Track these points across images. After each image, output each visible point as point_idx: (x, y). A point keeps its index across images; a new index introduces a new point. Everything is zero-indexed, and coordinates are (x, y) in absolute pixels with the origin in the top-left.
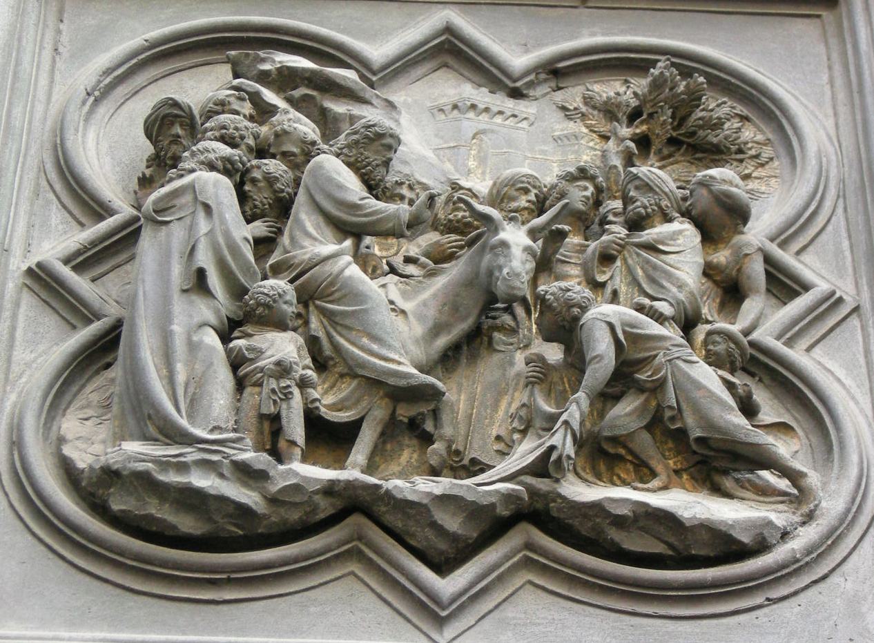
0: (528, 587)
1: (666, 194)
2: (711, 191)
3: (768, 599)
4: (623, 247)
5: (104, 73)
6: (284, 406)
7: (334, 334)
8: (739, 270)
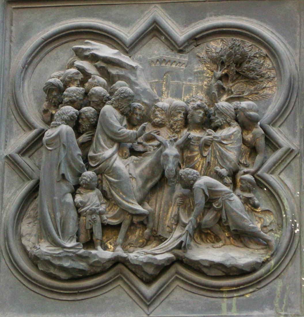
0: (178, 287)
1: (228, 115)
2: (244, 114)
3: (258, 288)
4: (212, 141)
5: (28, 56)
6: (94, 225)
7: (111, 189)
8: (255, 143)
